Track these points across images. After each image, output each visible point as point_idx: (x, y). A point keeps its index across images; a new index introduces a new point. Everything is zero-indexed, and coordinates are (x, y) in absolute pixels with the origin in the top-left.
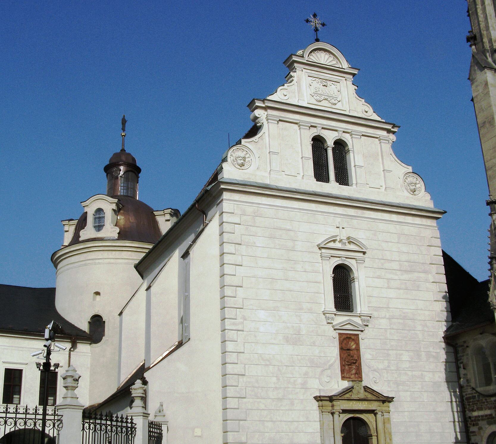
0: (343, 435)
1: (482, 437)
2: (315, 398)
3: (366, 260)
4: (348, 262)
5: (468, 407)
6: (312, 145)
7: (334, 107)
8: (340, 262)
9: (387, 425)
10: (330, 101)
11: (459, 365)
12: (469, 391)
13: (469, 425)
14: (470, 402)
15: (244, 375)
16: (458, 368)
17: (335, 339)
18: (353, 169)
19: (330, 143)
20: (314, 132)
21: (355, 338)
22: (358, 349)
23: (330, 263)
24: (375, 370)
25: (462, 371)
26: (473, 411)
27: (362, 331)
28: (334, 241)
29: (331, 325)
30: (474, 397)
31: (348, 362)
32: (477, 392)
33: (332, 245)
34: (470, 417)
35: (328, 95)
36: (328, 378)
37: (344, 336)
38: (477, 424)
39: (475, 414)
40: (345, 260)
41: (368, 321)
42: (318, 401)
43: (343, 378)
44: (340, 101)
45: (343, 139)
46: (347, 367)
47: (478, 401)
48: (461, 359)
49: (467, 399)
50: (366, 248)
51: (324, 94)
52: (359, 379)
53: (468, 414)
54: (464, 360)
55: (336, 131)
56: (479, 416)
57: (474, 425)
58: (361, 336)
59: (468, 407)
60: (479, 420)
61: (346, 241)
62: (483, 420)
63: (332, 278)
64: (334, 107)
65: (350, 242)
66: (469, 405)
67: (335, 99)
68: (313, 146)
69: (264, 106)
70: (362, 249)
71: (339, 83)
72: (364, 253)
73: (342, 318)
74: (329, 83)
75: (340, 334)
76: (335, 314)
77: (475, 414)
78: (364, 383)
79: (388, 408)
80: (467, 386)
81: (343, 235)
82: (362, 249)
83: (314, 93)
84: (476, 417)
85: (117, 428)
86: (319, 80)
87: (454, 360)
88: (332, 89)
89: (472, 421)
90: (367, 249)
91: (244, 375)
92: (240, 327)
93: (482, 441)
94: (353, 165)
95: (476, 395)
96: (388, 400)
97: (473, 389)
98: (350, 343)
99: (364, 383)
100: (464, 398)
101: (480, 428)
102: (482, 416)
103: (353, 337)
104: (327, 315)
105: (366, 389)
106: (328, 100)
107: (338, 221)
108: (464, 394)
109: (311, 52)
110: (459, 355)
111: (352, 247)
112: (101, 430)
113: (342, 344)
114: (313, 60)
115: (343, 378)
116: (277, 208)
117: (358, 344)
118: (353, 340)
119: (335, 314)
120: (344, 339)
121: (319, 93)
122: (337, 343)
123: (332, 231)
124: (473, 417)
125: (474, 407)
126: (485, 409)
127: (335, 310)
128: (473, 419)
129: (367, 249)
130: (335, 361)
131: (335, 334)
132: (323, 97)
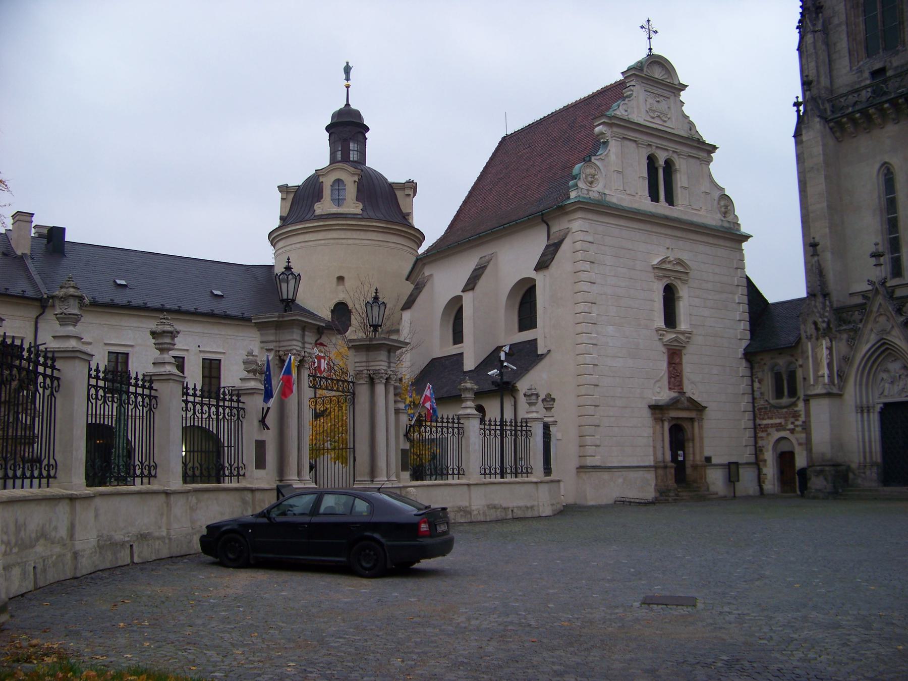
6: (648, 164)
8: (669, 282)
11: (754, 379)
12: (762, 402)
16: (753, 381)
18: (679, 190)
19: (661, 162)
22: (680, 364)
25: (756, 385)
26: (763, 419)
27: (684, 347)
30: (766, 408)
32: (769, 403)
34: (759, 425)
38: (766, 431)
41: (689, 338)
42: (651, 409)
43: (670, 389)
45: (673, 159)
46: (673, 379)
49: (758, 409)
53: (758, 421)
54: (760, 375)
57: (763, 431)
59: (759, 416)
60: (768, 427)
64: (665, 124)
65: (678, 263)
66: (760, 414)
69: (609, 122)
74: (662, 98)
75: (669, 350)
80: (760, 398)
84: (766, 425)
87: (750, 375)
88: (663, 106)
89: (761, 428)
90: (691, 270)
92: (594, 342)
94: (679, 185)
100: (756, 409)
101: (768, 434)
103: (677, 352)
104: (660, 332)
107: (668, 242)
108: (756, 405)
110: (754, 371)
111: (679, 268)
117: (681, 359)
121: (653, 109)
122: (665, 358)
124: (762, 425)
129: (691, 270)
130: (664, 374)
131: (664, 350)
132: (657, 113)
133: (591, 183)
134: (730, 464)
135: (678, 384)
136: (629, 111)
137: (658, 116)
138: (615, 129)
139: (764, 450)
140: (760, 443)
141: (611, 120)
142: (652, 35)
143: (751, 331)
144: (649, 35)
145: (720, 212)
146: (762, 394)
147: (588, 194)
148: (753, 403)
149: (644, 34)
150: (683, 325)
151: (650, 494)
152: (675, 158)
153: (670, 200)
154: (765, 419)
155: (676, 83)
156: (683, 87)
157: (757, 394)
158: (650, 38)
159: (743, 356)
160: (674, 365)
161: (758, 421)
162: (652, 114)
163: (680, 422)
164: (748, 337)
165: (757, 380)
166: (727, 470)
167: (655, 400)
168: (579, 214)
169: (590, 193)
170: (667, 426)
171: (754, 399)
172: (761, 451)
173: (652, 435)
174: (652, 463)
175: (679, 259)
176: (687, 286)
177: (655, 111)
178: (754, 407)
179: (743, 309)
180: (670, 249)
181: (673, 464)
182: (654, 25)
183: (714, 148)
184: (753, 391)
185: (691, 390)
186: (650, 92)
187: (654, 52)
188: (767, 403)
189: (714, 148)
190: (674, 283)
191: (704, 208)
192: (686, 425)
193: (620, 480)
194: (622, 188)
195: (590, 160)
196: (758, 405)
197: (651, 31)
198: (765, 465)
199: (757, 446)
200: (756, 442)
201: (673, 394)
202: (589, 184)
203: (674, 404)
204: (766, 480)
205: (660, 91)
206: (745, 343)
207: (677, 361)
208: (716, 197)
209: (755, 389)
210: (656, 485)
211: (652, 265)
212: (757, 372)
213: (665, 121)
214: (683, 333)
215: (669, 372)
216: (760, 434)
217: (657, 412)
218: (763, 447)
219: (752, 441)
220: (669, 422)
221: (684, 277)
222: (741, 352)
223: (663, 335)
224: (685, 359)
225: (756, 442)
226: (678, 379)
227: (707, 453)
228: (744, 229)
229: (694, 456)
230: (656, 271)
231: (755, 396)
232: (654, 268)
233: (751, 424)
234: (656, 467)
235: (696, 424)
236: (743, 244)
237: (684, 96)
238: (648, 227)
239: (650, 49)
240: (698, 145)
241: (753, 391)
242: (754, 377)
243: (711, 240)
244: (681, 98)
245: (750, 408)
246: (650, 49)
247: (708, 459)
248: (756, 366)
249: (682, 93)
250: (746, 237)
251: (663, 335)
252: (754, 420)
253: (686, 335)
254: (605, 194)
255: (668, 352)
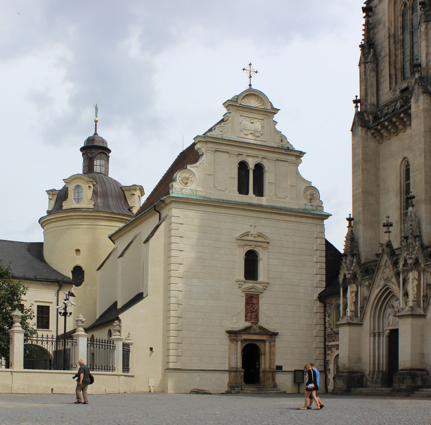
0: (243, 353)
1: (332, 356)
2: (227, 332)
3: (269, 247)
4: (256, 249)
5: (327, 339)
6: (238, 168)
7: (258, 139)
9: (273, 349)
10: (255, 135)
11: (326, 315)
13: (327, 350)
14: (329, 337)
15: (182, 317)
16: (325, 316)
17: (243, 297)
19: (251, 165)
20: (240, 159)
21: (257, 297)
22: (258, 303)
23: (243, 249)
24: (268, 316)
25: (327, 319)
26: (330, 342)
27: (261, 292)
28: (248, 235)
29: (241, 288)
30: (331, 334)
31: (250, 311)
32: (333, 331)
33: (246, 238)
34: (328, 346)
35: (254, 130)
36: (236, 320)
37: (249, 296)
38: (331, 350)
39: (331, 344)
40: (254, 248)
41: (266, 287)
42: (228, 333)
43: (246, 320)
44: (262, 134)
45: (262, 163)
46: (249, 314)
47: (333, 336)
48: (327, 311)
49: (328, 335)
50: (269, 240)
51: (251, 129)
52: (257, 322)
53: (327, 343)
54: (329, 311)
55: (257, 157)
56: (332, 345)
57: (329, 350)
58: (260, 296)
59: (327, 339)
60: (332, 347)
61: (256, 235)
62: (334, 347)
63: (244, 259)
66: (328, 338)
67: (259, 132)
68: (239, 169)
70: (267, 240)
71: (263, 120)
72: (268, 243)
73: (250, 284)
74: (255, 120)
75: (247, 295)
76: (244, 282)
77: (331, 344)
78: (259, 324)
79: (274, 339)
80: (329, 327)
81: (253, 231)
82: (267, 240)
83: (243, 129)
84: (331, 345)
85: (105, 346)
86: (248, 119)
87: (323, 312)
89: (329, 348)
91: (182, 317)
93: (332, 359)
95: (333, 333)
96: (276, 334)
97: (331, 329)
98: (253, 299)
99: (259, 324)
100: (326, 335)
101: (332, 352)
102: (334, 345)
103: (255, 296)
104: (238, 282)
105: (261, 328)
106: (253, 134)
107: (252, 222)
108: (326, 332)
109: (244, 97)
110: (327, 309)
111: (260, 239)
112: (97, 347)
113: (247, 300)
114: (246, 103)
115: (246, 320)
116: (210, 213)
118: (255, 298)
119: (244, 282)
120: (248, 298)
121: (247, 128)
122: (244, 300)
123: (246, 228)
124: (329, 345)
125: (330, 340)
126: (336, 341)
127: (244, 280)
128: (329, 346)
129: (270, 240)
130: (242, 311)
131: (243, 294)
132: (250, 131)
133: (186, 183)
134: (295, 371)
135: (254, 317)
136: (224, 132)
137: (251, 133)
138: (209, 145)
139: (329, 362)
140: (328, 358)
141: (205, 139)
142: (253, 74)
143: (326, 281)
144: (250, 75)
145: (306, 198)
146: (330, 325)
147: (181, 191)
148: (325, 331)
149: (246, 75)
150: (262, 276)
151: (225, 388)
152: (265, 163)
153: (259, 192)
154: (331, 342)
155: (269, 107)
156: (275, 111)
157: (327, 325)
158: (250, 77)
159: (317, 299)
160: (251, 305)
161: (327, 343)
162: (246, 132)
163: (254, 343)
164: (324, 285)
165: (327, 315)
166: (294, 375)
167: (231, 327)
168: (173, 205)
169: (183, 190)
170: (240, 346)
171: (325, 328)
172: (328, 363)
173: (228, 350)
174: (227, 369)
175: (260, 233)
176: (267, 251)
177: (249, 130)
178: (325, 333)
179: (319, 267)
180: (253, 226)
181: (243, 370)
182: (254, 67)
183: (300, 154)
184: (325, 322)
185: (264, 322)
186: (245, 116)
187: (253, 87)
188: (332, 331)
189: (300, 154)
190: (255, 249)
191: (289, 197)
192: (258, 344)
193: (198, 378)
194: (212, 186)
195: (186, 168)
196: (328, 332)
197: (252, 72)
198: (329, 373)
199: (326, 360)
200: (325, 358)
201: (248, 324)
202: (184, 185)
203: (246, 330)
204: (329, 383)
205: (255, 116)
206: (320, 290)
207: (255, 302)
208: (303, 188)
209: (327, 321)
210: (229, 383)
211: (236, 238)
212: (328, 309)
213: (258, 137)
214: (261, 283)
215: (246, 309)
216: (328, 352)
217: (232, 335)
218: (329, 360)
219: (322, 357)
220: (242, 341)
221: (265, 245)
222: (316, 295)
223: (242, 285)
224: (262, 301)
225: (325, 358)
226: (254, 314)
227: (278, 363)
228: (326, 210)
229: (265, 365)
230: (239, 241)
231: (326, 326)
232: (237, 239)
233: (322, 345)
234: (229, 371)
235: (267, 344)
236: (325, 221)
237: (276, 118)
238: (235, 212)
239: (250, 85)
240: (286, 152)
241: (325, 322)
242: (326, 313)
243: (293, 219)
244: (274, 119)
245: (322, 334)
246: (250, 85)
247: (279, 368)
248: (328, 305)
249: (275, 116)
250: (327, 216)
251: (242, 285)
252: (325, 342)
253: (263, 284)
254: (196, 191)
255: (246, 296)
